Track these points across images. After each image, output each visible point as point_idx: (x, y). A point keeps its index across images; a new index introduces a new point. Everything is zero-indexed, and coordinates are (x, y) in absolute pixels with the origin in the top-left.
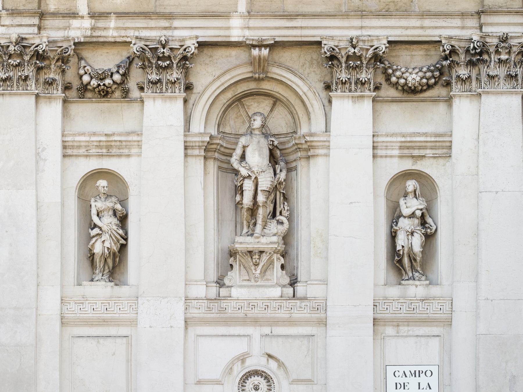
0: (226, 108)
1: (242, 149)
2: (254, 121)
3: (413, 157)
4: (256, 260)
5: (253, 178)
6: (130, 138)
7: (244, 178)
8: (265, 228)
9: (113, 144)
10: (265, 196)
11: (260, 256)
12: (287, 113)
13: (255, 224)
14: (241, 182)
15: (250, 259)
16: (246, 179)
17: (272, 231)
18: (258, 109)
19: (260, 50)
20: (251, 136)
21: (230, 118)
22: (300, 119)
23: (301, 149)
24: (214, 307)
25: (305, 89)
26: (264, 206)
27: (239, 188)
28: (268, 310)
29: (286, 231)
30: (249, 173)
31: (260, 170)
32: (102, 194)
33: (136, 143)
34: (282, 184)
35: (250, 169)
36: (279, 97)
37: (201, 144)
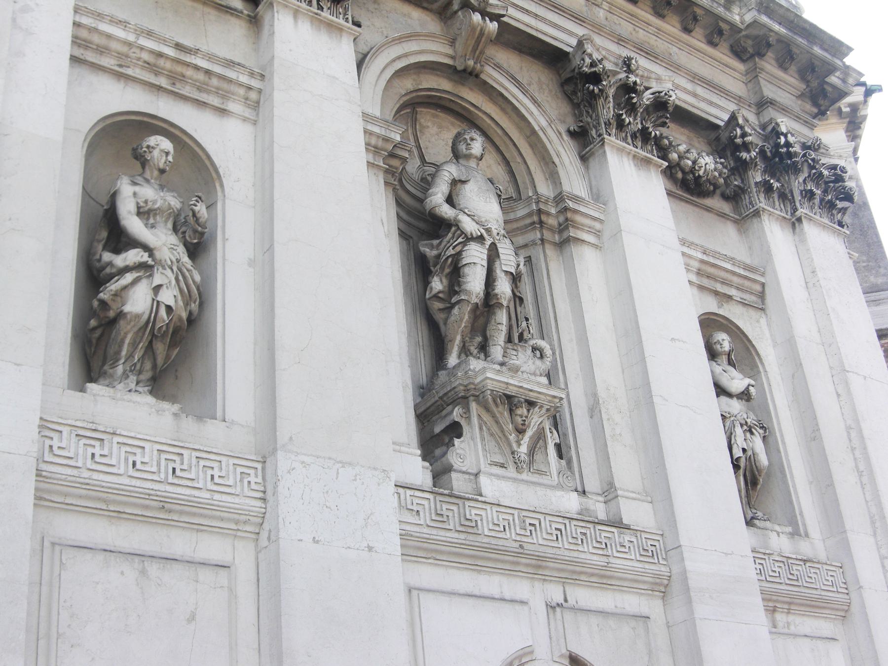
3: (716, 293)
4: (524, 418)
5: (488, 243)
6: (231, 74)
7: (469, 239)
9: (189, 72)
14: (458, 248)
15: (506, 414)
18: (436, 140)
19: (483, 18)
24: (450, 514)
25: (544, 123)
27: (450, 260)
28: (562, 540)
32: (156, 173)
33: (242, 91)
36: (489, 125)
37: (380, 143)
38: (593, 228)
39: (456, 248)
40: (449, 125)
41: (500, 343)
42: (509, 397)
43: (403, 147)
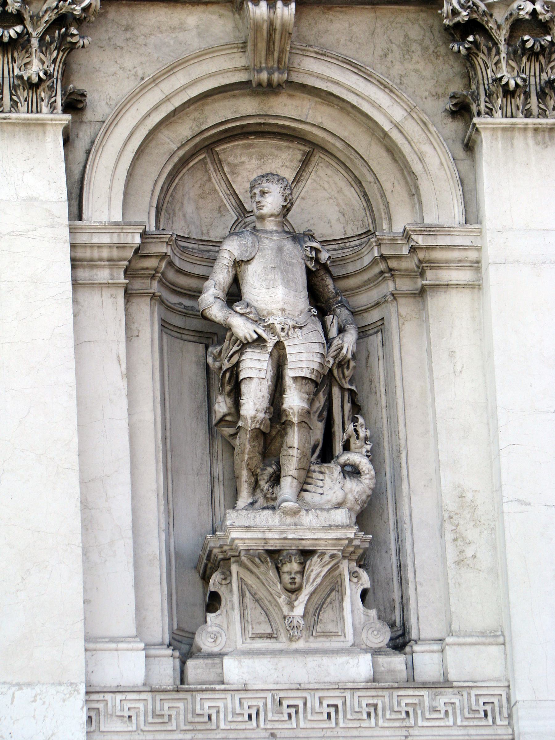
0: (176, 165)
1: (230, 270)
2: (262, 196)
4: (293, 576)
5: (270, 345)
7: (245, 345)
8: (306, 491)
10: (306, 396)
11: (303, 564)
13: (276, 479)
14: (235, 359)
15: (272, 573)
16: (248, 350)
17: (329, 498)
20: (257, 236)
21: (183, 195)
22: (388, 194)
23: (397, 273)
24: (173, 713)
25: (398, 114)
26: (304, 425)
27: (228, 375)
28: (337, 719)
29: (368, 496)
30: (260, 331)
31: (291, 323)
34: (348, 368)
35: (259, 320)
36: (323, 139)
37: (115, 253)
38: (467, 261)
39: (232, 359)
40: (273, 150)
41: (291, 473)
42: (271, 553)
43: (158, 240)
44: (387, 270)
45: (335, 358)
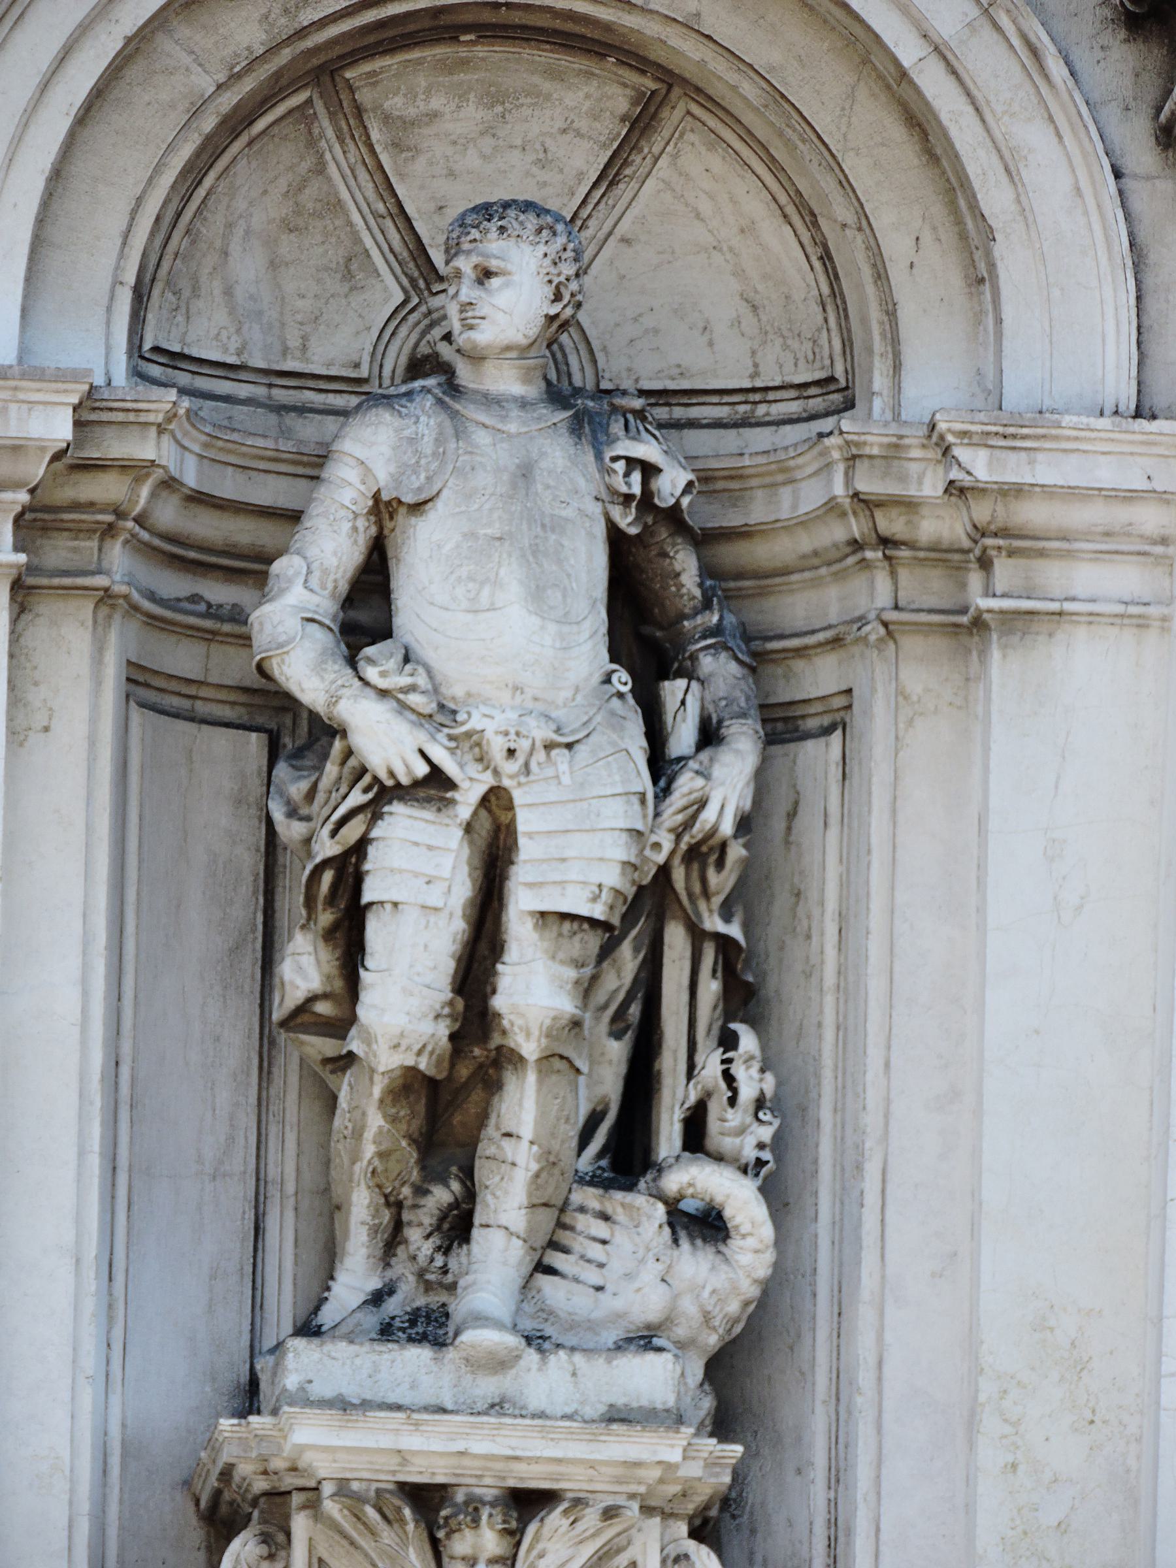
0: (208, 139)
1: (361, 523)
2: (480, 282)
5: (468, 798)
8: (551, 1271)
10: (571, 974)
11: (514, 1535)
12: (757, 207)
14: (353, 832)
16: (397, 808)
17: (618, 1304)
18: (484, 157)
20: (454, 415)
21: (230, 226)
22: (897, 273)
23: (904, 553)
26: (558, 1064)
29: (746, 1304)
30: (440, 756)
31: (542, 732)
34: (720, 864)
38: (1129, 535)
39: (344, 831)
40: (536, 79)
41: (504, 1219)
43: (131, 417)
44: (873, 538)
45: (678, 833)
